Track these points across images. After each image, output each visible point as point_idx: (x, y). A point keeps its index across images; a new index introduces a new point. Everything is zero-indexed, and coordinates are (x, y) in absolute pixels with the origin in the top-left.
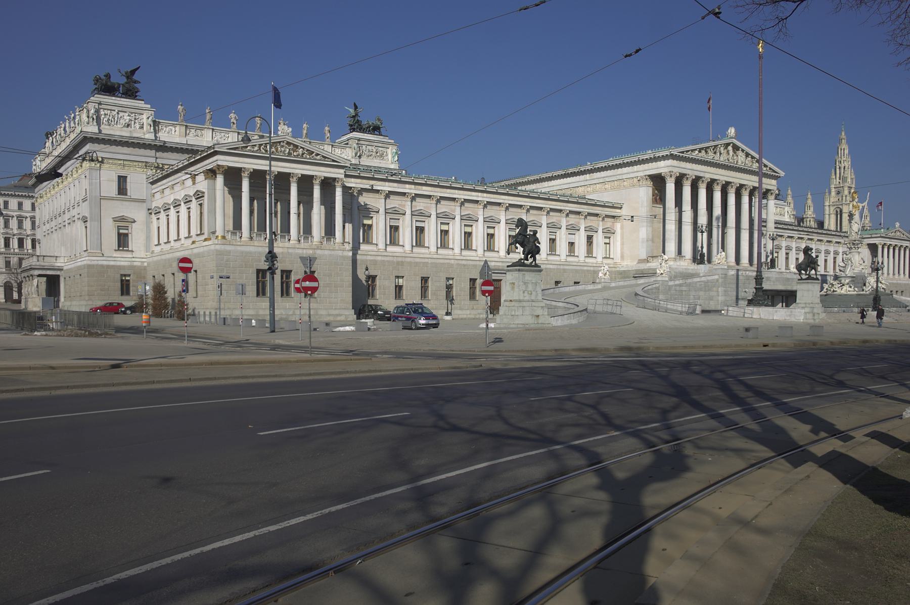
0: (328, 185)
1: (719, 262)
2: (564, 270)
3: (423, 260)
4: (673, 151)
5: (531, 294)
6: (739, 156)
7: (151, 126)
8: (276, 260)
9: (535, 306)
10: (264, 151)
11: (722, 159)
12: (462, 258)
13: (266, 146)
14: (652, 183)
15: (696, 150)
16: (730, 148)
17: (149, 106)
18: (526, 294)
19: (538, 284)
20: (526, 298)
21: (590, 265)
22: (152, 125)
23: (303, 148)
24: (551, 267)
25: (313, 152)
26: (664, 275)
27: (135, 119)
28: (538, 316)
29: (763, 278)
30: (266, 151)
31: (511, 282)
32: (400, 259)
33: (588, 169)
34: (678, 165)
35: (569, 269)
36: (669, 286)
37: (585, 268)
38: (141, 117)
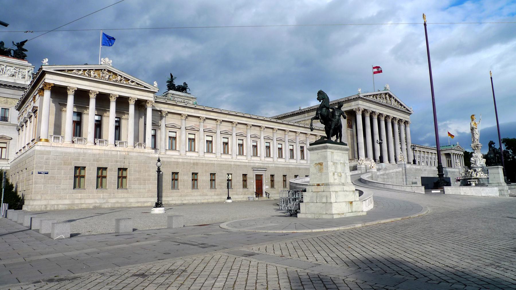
0: (141, 105)
1: (401, 160)
3: (212, 162)
4: (361, 95)
5: (341, 176)
6: (392, 101)
7: (30, 76)
10: (87, 75)
13: (90, 72)
16: (387, 96)
17: (31, 64)
18: (336, 176)
19: (345, 164)
20: (337, 181)
22: (31, 76)
23: (121, 76)
24: (292, 166)
25: (129, 80)
27: (19, 72)
28: (351, 203)
30: (90, 75)
31: (317, 162)
32: (195, 161)
33: (306, 111)
35: (302, 168)
36: (377, 175)
38: (24, 71)
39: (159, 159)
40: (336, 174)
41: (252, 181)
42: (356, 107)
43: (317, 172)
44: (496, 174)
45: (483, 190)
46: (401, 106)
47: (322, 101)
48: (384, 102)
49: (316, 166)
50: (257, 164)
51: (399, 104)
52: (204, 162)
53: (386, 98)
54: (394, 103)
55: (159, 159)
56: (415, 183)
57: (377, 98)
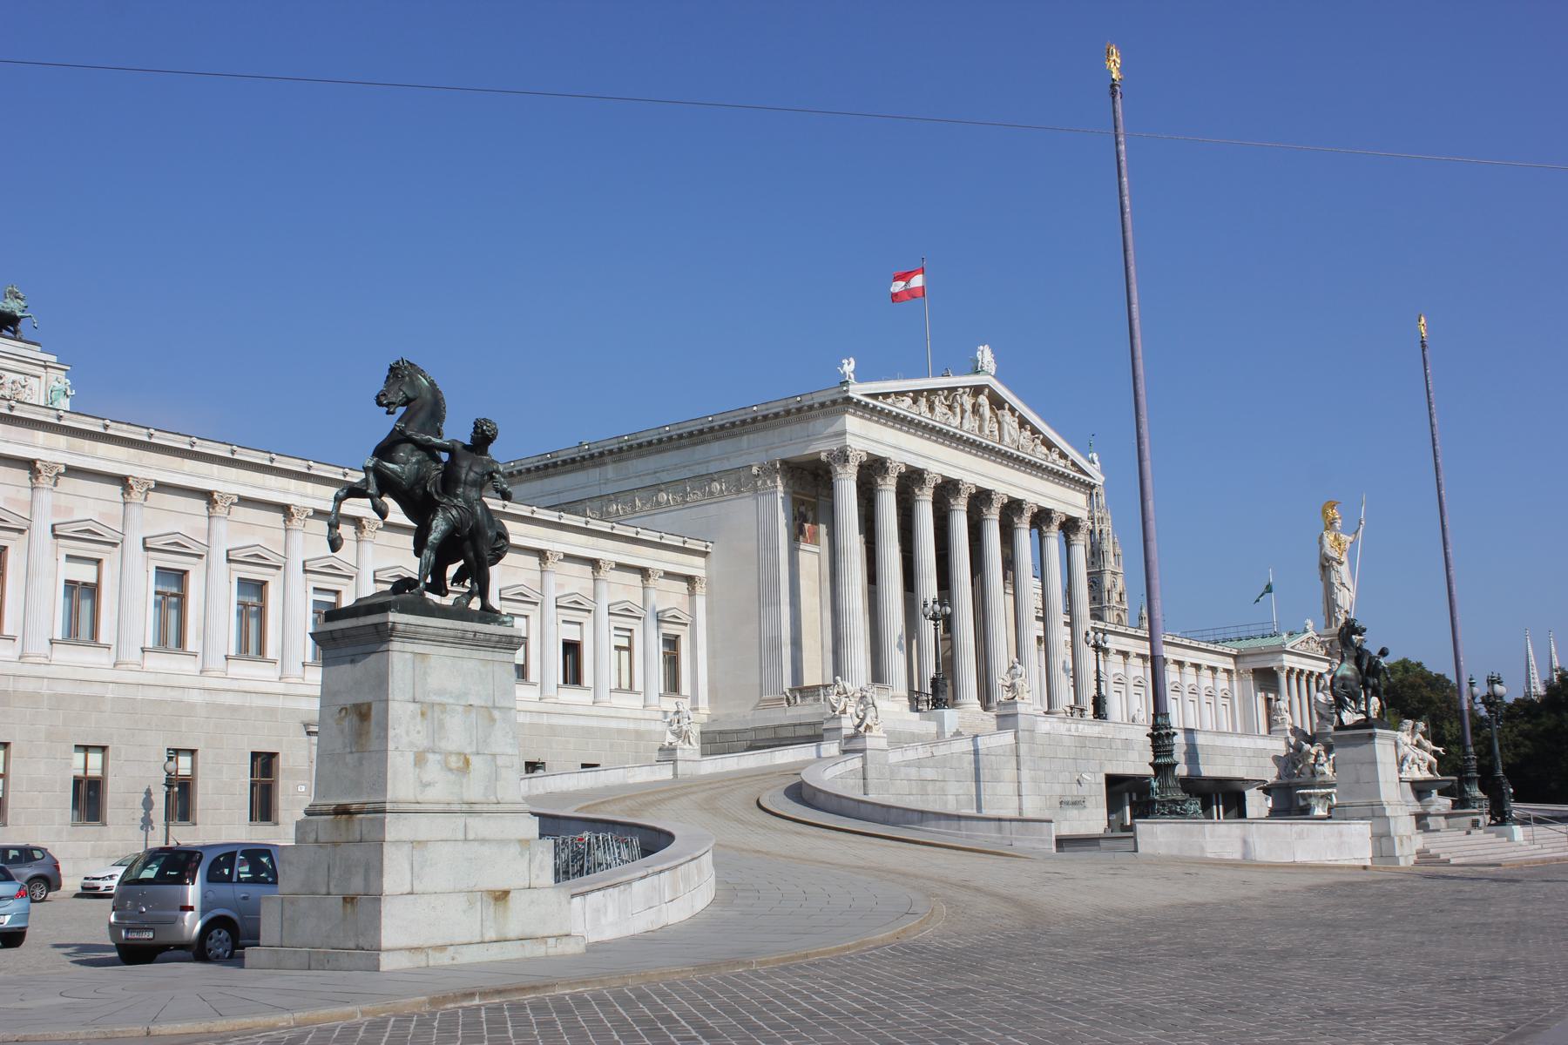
2: (552, 728)
3: (86, 690)
6: (1006, 426)
9: (483, 841)
11: (966, 427)
12: (226, 684)
14: (791, 483)
16: (983, 399)
18: (433, 769)
19: (497, 714)
21: (626, 713)
26: (875, 732)
28: (502, 896)
31: (349, 700)
34: (863, 433)
37: (613, 724)
40: (431, 756)
42: (834, 446)
43: (345, 747)
44: (1363, 764)
45: (1300, 836)
46: (1044, 450)
47: (401, 410)
48: (965, 427)
49: (342, 719)
51: (1039, 442)
52: (44, 688)
54: (1012, 432)
56: (1074, 803)
57: (931, 408)
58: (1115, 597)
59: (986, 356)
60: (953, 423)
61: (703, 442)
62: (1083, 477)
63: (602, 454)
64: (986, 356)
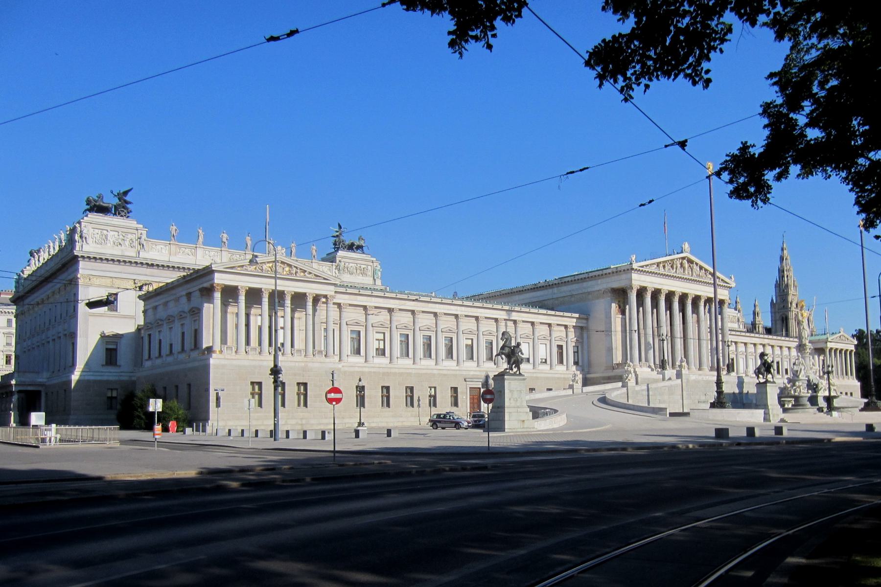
3: (407, 371)
5: (517, 400)
8: (281, 373)
15: (654, 264)
16: (685, 261)
19: (522, 391)
23: (297, 268)
25: (305, 271)
28: (523, 421)
29: (723, 382)
32: (386, 370)
36: (636, 391)
37: (556, 376)
39: (360, 378)
40: (512, 399)
41: (464, 397)
50: (472, 373)
51: (708, 274)
52: (397, 371)
53: (682, 264)
55: (360, 378)
57: (664, 267)
58: (794, 305)
59: (686, 246)
60: (672, 272)
61: (587, 281)
62: (726, 285)
63: (552, 285)
64: (686, 246)
